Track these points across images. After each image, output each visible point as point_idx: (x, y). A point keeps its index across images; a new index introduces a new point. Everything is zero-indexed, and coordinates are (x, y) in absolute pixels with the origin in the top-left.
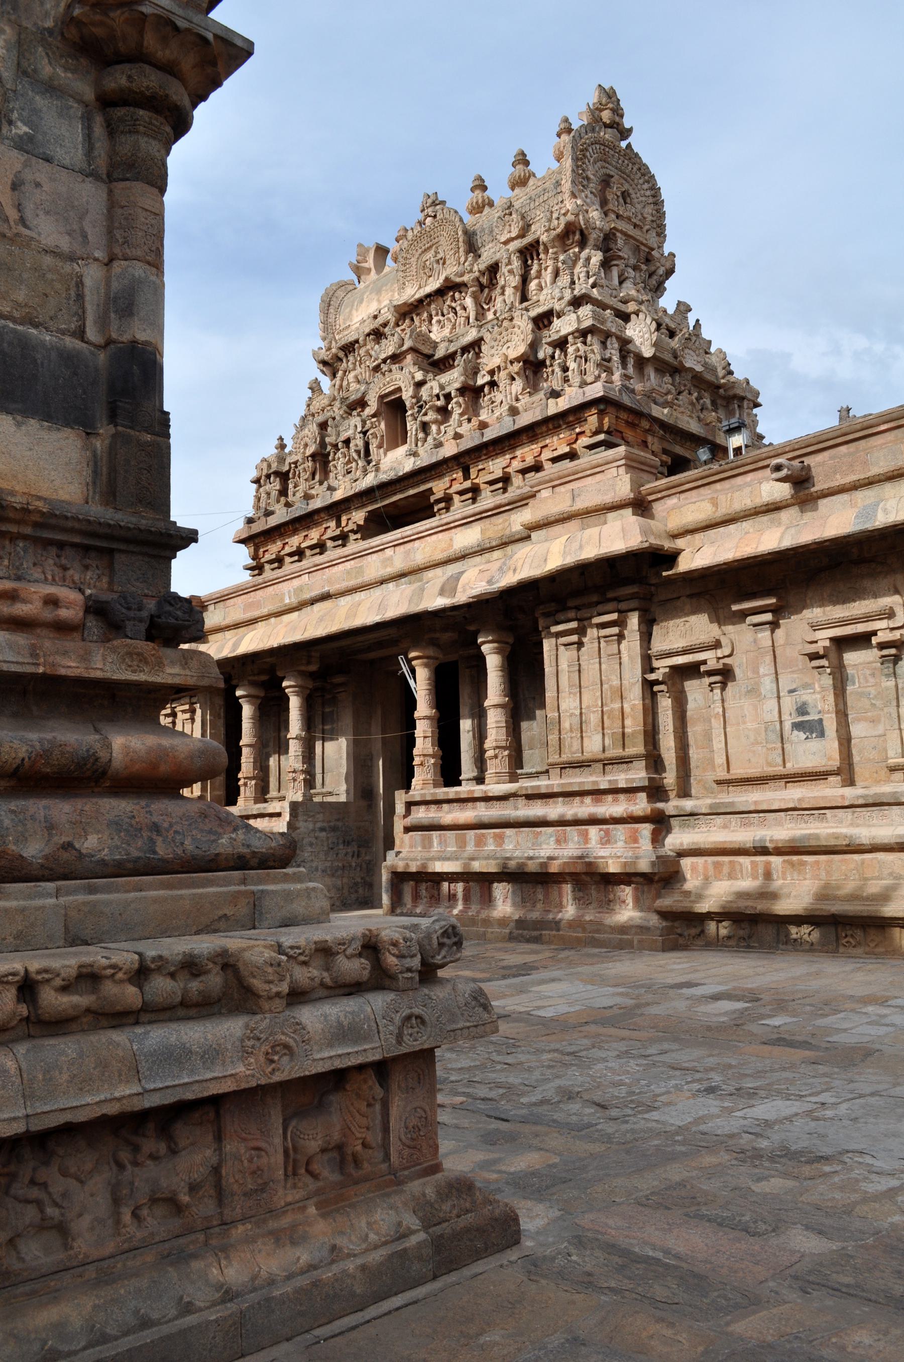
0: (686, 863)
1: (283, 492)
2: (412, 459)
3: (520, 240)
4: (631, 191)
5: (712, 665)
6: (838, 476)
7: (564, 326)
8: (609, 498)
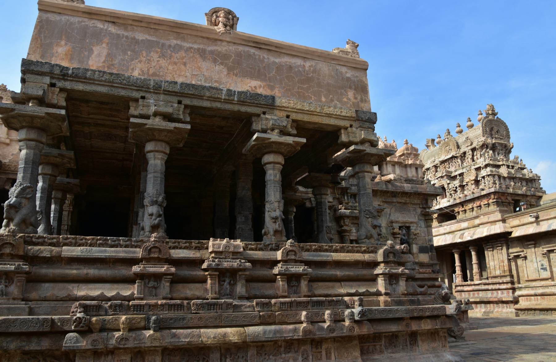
0: (520, 299)
5: (523, 255)
8: (496, 219)
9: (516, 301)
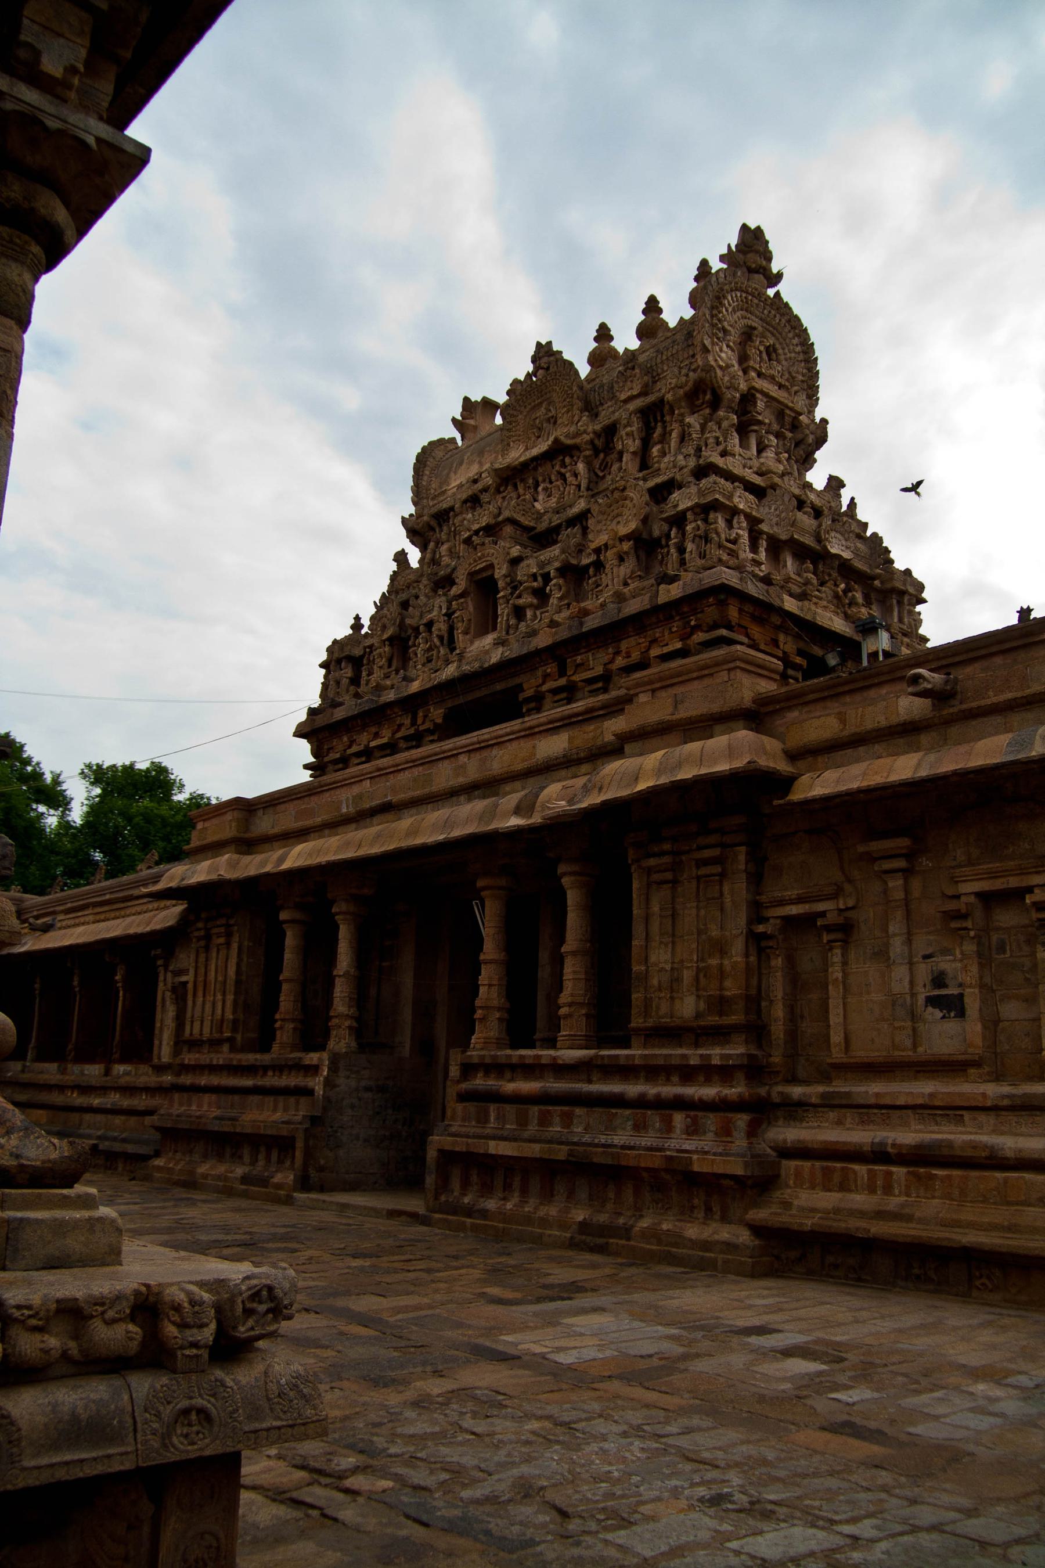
1: (355, 681)
2: (501, 649)
3: (642, 399)
4: (777, 346)
5: (832, 918)
6: (991, 693)
7: (683, 500)
9: (761, 1183)
